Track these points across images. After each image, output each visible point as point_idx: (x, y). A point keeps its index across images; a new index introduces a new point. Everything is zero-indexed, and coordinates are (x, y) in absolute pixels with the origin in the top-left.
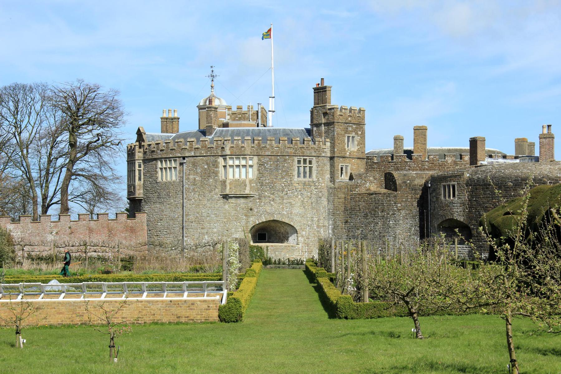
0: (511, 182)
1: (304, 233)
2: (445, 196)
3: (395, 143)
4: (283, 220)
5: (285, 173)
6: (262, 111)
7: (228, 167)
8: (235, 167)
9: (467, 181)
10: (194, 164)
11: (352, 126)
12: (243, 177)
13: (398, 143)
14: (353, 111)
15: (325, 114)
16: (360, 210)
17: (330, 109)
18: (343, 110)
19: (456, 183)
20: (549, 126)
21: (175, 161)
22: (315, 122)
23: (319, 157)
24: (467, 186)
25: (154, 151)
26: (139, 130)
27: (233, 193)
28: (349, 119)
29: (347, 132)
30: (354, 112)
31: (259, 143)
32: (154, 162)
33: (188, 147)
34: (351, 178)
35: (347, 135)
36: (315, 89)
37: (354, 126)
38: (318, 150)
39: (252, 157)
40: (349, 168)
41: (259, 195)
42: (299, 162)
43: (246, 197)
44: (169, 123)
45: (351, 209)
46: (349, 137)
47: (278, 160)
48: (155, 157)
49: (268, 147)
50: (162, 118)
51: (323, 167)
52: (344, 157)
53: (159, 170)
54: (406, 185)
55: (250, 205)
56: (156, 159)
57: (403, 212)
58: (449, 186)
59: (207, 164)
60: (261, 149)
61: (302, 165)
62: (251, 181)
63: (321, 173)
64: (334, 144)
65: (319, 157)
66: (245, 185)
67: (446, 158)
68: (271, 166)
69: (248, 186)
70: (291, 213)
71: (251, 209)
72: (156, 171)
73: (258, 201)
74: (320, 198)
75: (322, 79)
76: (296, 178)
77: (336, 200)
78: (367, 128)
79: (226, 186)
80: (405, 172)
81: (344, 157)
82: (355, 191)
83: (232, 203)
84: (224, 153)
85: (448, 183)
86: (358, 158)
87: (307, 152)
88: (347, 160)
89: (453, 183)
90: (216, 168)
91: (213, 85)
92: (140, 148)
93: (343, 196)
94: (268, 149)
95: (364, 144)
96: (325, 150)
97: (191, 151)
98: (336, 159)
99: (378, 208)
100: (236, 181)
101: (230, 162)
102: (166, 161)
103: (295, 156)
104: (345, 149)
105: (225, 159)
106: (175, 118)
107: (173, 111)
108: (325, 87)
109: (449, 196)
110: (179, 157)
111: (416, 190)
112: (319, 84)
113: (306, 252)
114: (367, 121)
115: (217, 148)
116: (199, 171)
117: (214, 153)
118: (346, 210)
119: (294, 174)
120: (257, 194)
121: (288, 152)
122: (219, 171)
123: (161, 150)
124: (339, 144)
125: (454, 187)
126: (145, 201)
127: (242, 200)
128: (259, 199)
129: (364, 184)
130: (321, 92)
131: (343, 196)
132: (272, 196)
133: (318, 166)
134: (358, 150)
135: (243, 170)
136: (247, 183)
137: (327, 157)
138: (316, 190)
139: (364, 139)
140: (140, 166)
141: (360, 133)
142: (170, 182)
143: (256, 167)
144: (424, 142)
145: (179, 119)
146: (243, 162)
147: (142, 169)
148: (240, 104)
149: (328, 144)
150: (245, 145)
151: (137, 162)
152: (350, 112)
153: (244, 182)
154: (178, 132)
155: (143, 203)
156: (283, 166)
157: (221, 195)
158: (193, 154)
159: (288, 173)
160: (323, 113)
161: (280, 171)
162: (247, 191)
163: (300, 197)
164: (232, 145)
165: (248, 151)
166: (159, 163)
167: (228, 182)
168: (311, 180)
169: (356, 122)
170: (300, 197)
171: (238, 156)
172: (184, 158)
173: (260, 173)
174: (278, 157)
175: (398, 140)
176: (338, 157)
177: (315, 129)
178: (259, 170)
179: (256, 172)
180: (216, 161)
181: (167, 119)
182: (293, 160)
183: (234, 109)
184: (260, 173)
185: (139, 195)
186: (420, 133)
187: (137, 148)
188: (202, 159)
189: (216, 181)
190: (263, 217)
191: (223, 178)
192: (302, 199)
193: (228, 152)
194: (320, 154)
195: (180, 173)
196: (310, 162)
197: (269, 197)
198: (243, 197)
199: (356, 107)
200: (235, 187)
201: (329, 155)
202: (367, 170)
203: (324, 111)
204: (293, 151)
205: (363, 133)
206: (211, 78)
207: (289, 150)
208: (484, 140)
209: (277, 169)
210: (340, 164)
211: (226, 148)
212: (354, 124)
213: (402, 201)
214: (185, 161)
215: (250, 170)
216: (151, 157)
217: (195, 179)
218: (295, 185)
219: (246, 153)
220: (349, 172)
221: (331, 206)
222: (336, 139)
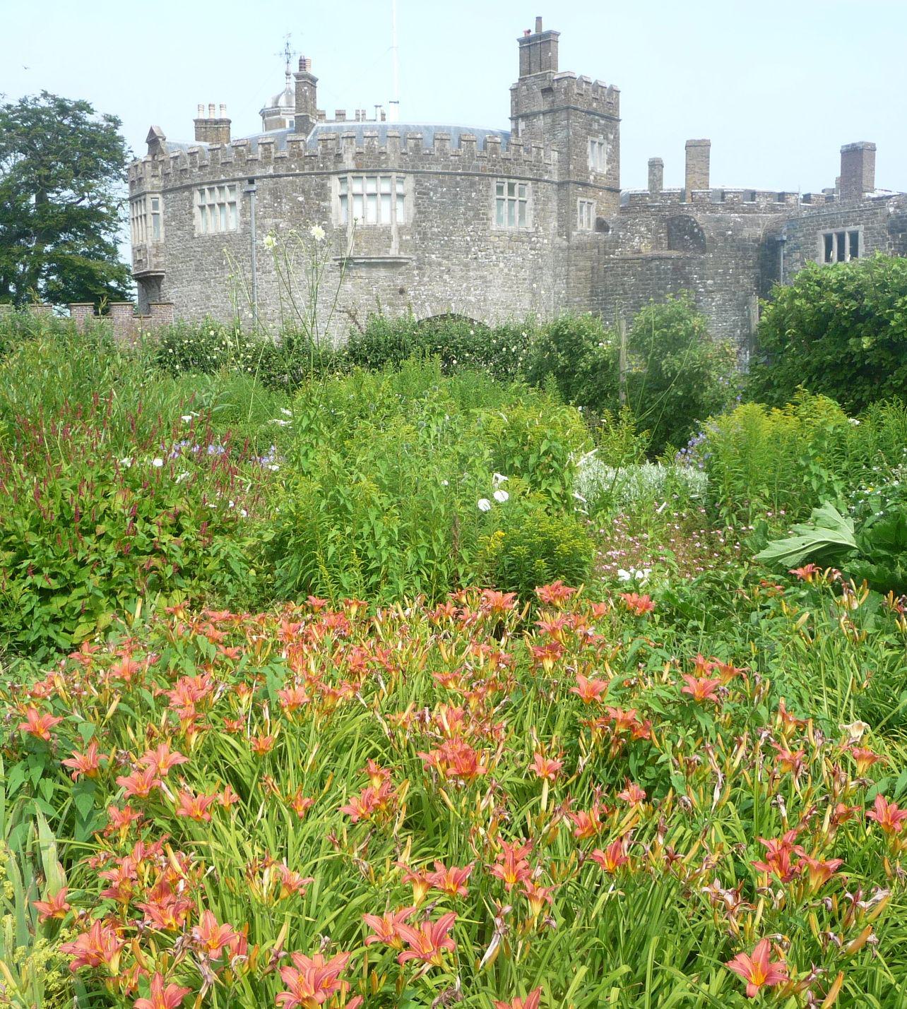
2: (828, 259)
3: (651, 173)
5: (472, 213)
7: (350, 196)
8: (365, 196)
9: (892, 223)
10: (276, 195)
12: (385, 220)
13: (656, 171)
15: (547, 91)
16: (626, 293)
17: (558, 80)
21: (232, 188)
22: (524, 111)
23: (538, 180)
24: (891, 232)
25: (186, 170)
26: (152, 132)
27: (362, 255)
29: (590, 132)
30: (603, 92)
31: (416, 145)
32: (186, 194)
33: (259, 157)
34: (601, 226)
35: (590, 138)
36: (521, 41)
37: (602, 122)
38: (537, 165)
39: (402, 175)
40: (593, 209)
41: (418, 259)
42: (500, 189)
43: (394, 264)
44: (211, 128)
45: (606, 291)
46: (593, 142)
47: (457, 183)
48: (187, 182)
49: (437, 154)
50: (196, 121)
51: (545, 204)
52: (585, 185)
53: (196, 210)
54: (726, 239)
55: (400, 281)
56: (188, 187)
57: (718, 297)
58: (841, 238)
59: (303, 192)
60: (421, 159)
61: (505, 195)
62: (400, 229)
63: (540, 217)
64: (569, 155)
65: (538, 180)
66: (390, 238)
67: (757, 200)
68: (442, 193)
70: (485, 300)
71: (402, 291)
72: (190, 213)
73: (416, 272)
74: (540, 268)
75: (539, 19)
76: (494, 226)
77: (572, 274)
78: (622, 127)
82: (613, 254)
83: (361, 277)
84: (341, 167)
85: (840, 230)
87: (516, 170)
89: (852, 228)
90: (324, 200)
92: (155, 167)
93: (589, 264)
94: (437, 160)
95: (618, 162)
96: (550, 168)
97: (267, 164)
98: (571, 186)
99: (665, 289)
100: (369, 228)
101: (357, 187)
102: (211, 190)
103: (493, 176)
104: (587, 168)
105: (343, 181)
106: (221, 121)
107: (217, 107)
108: (549, 33)
109: (841, 257)
110: (240, 180)
111: (745, 249)
112: (529, 31)
114: (622, 114)
115: (325, 155)
116: (286, 208)
117: (318, 168)
118: (594, 293)
119: (490, 216)
120: (414, 258)
121: (477, 167)
122: (330, 207)
123: (202, 167)
124: (577, 155)
125: (854, 237)
126: (170, 280)
127: (382, 273)
128: (419, 268)
129: (630, 240)
130: (537, 48)
131: (589, 264)
132: (445, 262)
133: (536, 202)
135: (385, 204)
136: (394, 232)
137: (552, 183)
138: (533, 252)
140: (155, 205)
141: (611, 137)
142: (222, 236)
143: (410, 199)
144: (704, 171)
145: (229, 122)
146: (385, 187)
147: (160, 211)
148: (340, 108)
149: (555, 155)
150: (388, 148)
151: (148, 197)
152: (595, 91)
153: (386, 233)
155: (165, 285)
156: (469, 199)
157: (335, 260)
158: (271, 171)
159: (478, 215)
161: (462, 209)
162: (393, 252)
163: (502, 265)
164: (361, 150)
165: (394, 162)
166: (197, 195)
167: (350, 230)
168: (522, 229)
170: (502, 265)
171: (372, 174)
172: (251, 181)
173: (419, 212)
174: (458, 178)
175: (655, 167)
176: (575, 183)
177: (522, 125)
178: (417, 205)
179: (412, 210)
180: (324, 186)
181: (206, 121)
182: (488, 186)
184: (419, 212)
185: (156, 266)
186: (698, 152)
187: (148, 167)
188: (292, 182)
190: (428, 308)
191: (342, 221)
193: (349, 163)
194: (541, 175)
195: (243, 215)
196: (521, 193)
197: (440, 264)
198: (385, 265)
200: (367, 242)
201: (556, 178)
203: (546, 84)
204: (489, 166)
205: (617, 139)
206: (291, 51)
207: (480, 164)
208: (872, 149)
209: (455, 203)
210: (579, 199)
211: (345, 156)
212: (602, 117)
213: (717, 273)
214: (254, 187)
215: (400, 205)
216: (178, 184)
217: (277, 226)
219: (390, 166)
220: (593, 216)
221: (561, 285)
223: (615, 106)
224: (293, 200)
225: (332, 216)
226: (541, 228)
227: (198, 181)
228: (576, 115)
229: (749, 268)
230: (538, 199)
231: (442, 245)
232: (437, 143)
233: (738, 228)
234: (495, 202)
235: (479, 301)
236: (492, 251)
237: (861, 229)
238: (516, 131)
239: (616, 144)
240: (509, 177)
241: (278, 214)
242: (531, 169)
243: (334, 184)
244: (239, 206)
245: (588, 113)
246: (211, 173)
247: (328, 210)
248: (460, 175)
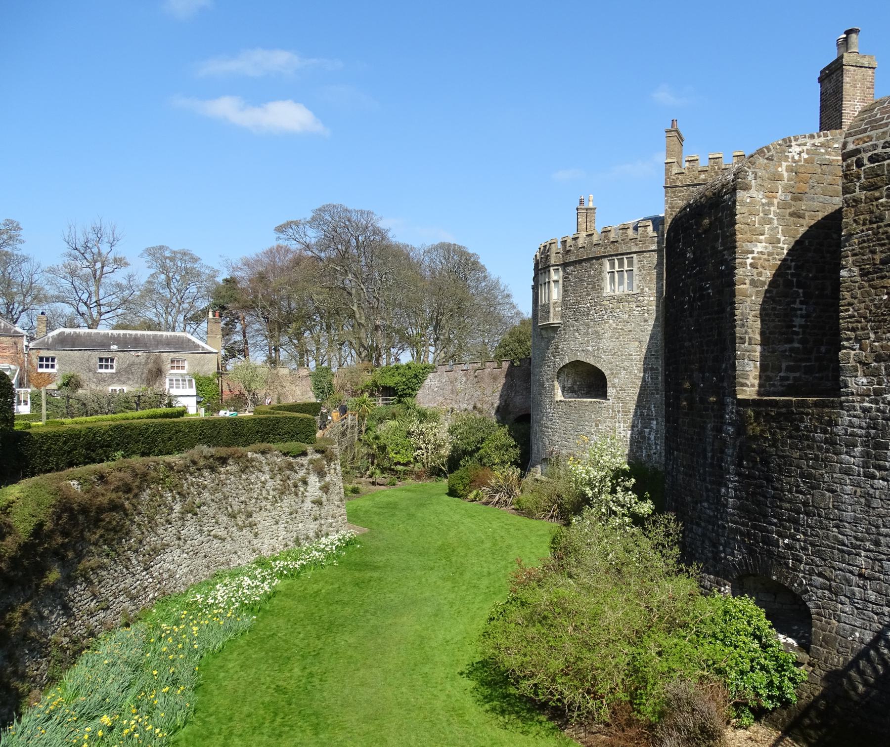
1: (616, 380)
4: (588, 361)
5: (590, 286)
28: (703, 176)
69: (552, 311)
70: (598, 349)
74: (646, 321)
87: (623, 249)
113: (619, 412)
143: (561, 282)
156: (589, 276)
159: (596, 286)
170: (611, 321)
182: (601, 264)
192: (614, 325)
196: (631, 263)
204: (602, 250)
207: (597, 249)
218: (605, 303)
226: (646, 289)
228: (674, 192)
230: (643, 267)
235: (594, 350)
236: (604, 312)
240: (617, 255)
242: (637, 245)
248: (585, 260)
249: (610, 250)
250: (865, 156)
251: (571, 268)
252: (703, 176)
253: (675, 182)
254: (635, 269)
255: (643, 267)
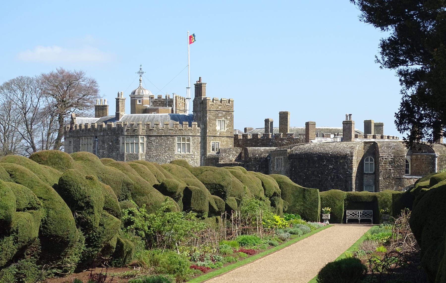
0: (317, 157)
3: (266, 124)
6: (176, 99)
10: (103, 143)
11: (222, 113)
14: (223, 102)
18: (214, 101)
19: (283, 157)
20: (350, 115)
28: (220, 107)
29: (217, 117)
35: (217, 119)
42: (179, 140)
52: (215, 136)
53: (81, 145)
56: (79, 137)
59: (111, 141)
75: (200, 78)
76: (176, 152)
78: (234, 113)
79: (124, 158)
80: (257, 148)
81: (215, 136)
86: (227, 137)
88: (218, 138)
90: (118, 144)
91: (141, 80)
94: (155, 131)
97: (101, 131)
103: (176, 136)
104: (216, 130)
124: (210, 126)
125: (281, 159)
129: (228, 156)
130: (199, 88)
134: (227, 131)
139: (233, 122)
154: (106, 115)
159: (171, 149)
160: (200, 103)
167: (125, 155)
169: (227, 110)
172: (96, 137)
173: (149, 149)
174: (163, 137)
180: (118, 139)
181: (99, 106)
182: (174, 139)
183: (156, 97)
186: (284, 117)
188: (108, 138)
189: (118, 155)
194: (196, 134)
195: (94, 148)
196: (189, 140)
199: (226, 98)
202: (234, 146)
207: (171, 131)
208: (314, 124)
210: (211, 142)
214: (97, 139)
217: (103, 152)
222: (207, 122)
223: (232, 106)
224: (108, 144)
225: (120, 150)
226: (196, 153)
227: (81, 135)
229: (264, 168)
230: (195, 143)
231: (156, 160)
232: (155, 126)
233: (262, 153)
234: (177, 145)
237: (283, 157)
238: (193, 116)
239: (232, 120)
240: (182, 136)
241: (104, 149)
243: (121, 139)
244: (92, 145)
245: (217, 111)
246: (85, 133)
247: (119, 147)
248: (163, 136)
249: (178, 133)
250: (384, 158)
251: (153, 138)
252: (220, 107)
253: (210, 108)
254: (191, 143)
255: (195, 143)
